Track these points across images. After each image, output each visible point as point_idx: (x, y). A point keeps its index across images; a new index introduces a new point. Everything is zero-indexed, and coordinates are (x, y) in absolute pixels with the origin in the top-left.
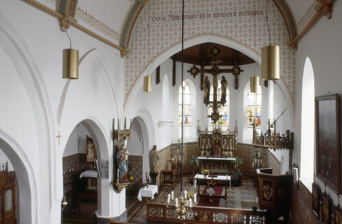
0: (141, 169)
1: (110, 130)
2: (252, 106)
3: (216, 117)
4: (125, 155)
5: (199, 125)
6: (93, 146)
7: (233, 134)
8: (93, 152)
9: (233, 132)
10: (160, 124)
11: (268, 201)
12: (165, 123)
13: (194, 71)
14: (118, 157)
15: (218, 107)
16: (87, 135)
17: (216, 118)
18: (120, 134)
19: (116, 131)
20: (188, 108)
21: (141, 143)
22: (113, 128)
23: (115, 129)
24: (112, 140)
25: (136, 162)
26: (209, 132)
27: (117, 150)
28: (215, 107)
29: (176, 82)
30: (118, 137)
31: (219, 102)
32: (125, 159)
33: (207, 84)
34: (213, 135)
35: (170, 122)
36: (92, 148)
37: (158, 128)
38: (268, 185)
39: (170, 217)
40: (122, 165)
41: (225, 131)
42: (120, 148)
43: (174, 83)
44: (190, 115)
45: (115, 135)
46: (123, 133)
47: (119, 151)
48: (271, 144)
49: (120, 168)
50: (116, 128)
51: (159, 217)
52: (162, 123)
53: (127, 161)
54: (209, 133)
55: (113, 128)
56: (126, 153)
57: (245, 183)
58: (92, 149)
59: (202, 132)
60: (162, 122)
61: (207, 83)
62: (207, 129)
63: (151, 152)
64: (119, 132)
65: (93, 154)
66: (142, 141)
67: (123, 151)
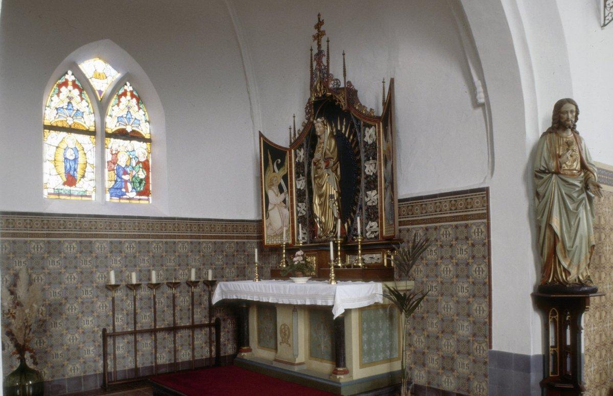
0: (483, 267)
6: (285, 178)
8: (284, 201)
16: (261, 135)
21: (479, 111)
25: (456, 227)
37: (599, 28)
63: (536, 152)
65: (286, 212)
66: (481, 99)
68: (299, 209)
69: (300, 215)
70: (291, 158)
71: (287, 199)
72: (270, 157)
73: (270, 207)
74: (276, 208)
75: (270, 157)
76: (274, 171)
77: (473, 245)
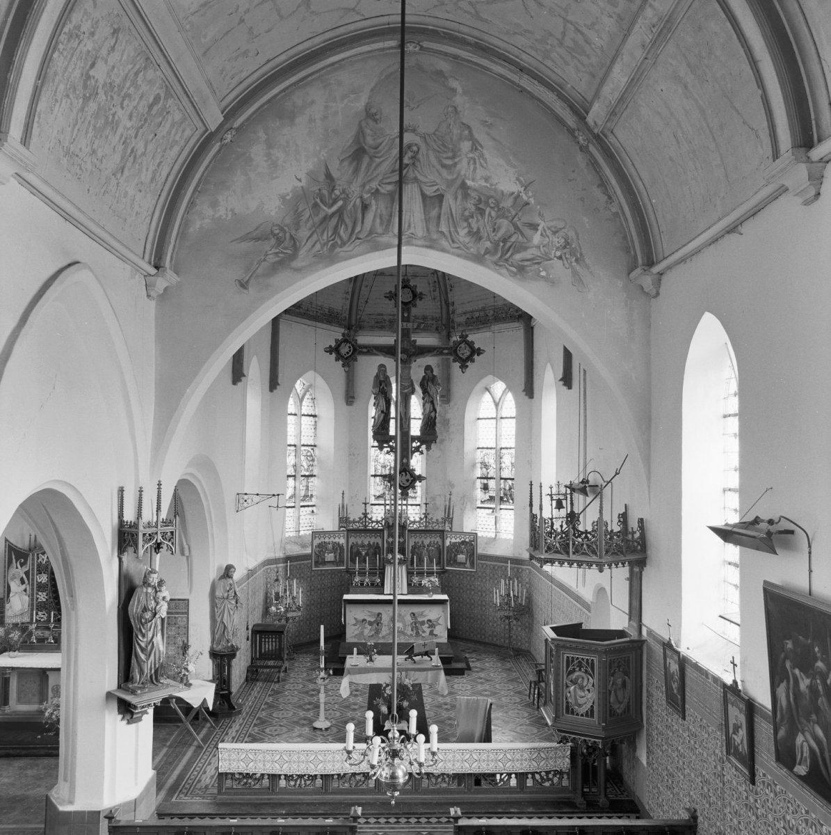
1: (112, 520)
2: (490, 450)
3: (408, 481)
4: (157, 603)
5: (343, 500)
6: (27, 573)
7: (440, 528)
8: (25, 590)
9: (440, 520)
10: (241, 501)
11: (582, 715)
12: (256, 499)
13: (345, 350)
14: (134, 608)
15: (413, 452)
16: (6, 540)
17: (408, 484)
18: (144, 535)
19: (130, 527)
20: (309, 454)
22: (121, 515)
23: (125, 519)
24: (116, 554)
26: (373, 522)
27: (128, 590)
28: (406, 454)
29: (281, 379)
30: (136, 545)
31: (414, 439)
32: (157, 616)
33: (383, 388)
34: (385, 532)
35: (274, 495)
36: (24, 577)
38: (580, 670)
39: (292, 783)
40: (150, 635)
41: (418, 519)
42: (138, 581)
43: (273, 384)
44: (315, 476)
45: (126, 537)
46: (154, 530)
47: (138, 590)
48: (590, 554)
49: (143, 645)
50: (129, 516)
51: (257, 786)
52: (246, 497)
53: (163, 620)
54: (374, 524)
55: (121, 515)
56: (161, 595)
57: (478, 664)
58: (23, 582)
59: (354, 522)
60: (246, 494)
61: (383, 385)
62: (365, 515)
64: (141, 528)
65: (26, 598)
66: (187, 553)
67: (150, 590)
68: (38, 596)
69: (39, 600)
70: (33, 559)
71: (28, 589)
72: (13, 557)
73: (11, 595)
74: (17, 595)
75: (13, 557)
76: (17, 568)
77: (179, 628)
